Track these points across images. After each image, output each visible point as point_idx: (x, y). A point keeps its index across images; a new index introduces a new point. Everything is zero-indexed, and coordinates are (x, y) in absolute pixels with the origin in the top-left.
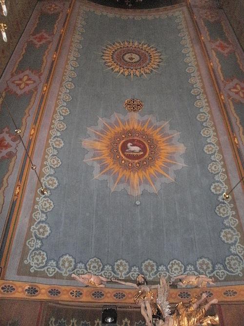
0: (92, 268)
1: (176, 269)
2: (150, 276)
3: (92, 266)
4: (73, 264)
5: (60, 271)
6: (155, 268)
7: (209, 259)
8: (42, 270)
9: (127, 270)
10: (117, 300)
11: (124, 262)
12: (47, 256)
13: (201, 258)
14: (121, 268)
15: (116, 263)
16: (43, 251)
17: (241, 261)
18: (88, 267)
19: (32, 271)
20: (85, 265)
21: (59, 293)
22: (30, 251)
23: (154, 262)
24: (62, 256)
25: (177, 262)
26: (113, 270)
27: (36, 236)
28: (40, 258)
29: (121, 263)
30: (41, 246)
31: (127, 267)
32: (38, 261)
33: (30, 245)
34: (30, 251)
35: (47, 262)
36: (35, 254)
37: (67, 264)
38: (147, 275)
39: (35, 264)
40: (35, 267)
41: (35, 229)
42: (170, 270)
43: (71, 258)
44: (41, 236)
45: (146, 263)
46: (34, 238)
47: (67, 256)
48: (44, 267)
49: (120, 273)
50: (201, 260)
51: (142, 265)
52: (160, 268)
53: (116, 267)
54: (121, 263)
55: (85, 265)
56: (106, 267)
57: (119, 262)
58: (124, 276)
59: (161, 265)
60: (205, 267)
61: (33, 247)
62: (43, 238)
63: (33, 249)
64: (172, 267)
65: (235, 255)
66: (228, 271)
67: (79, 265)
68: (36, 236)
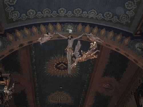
0: (45, 13)
1: (93, 14)
2: (77, 15)
3: (45, 12)
4: (35, 13)
5: (28, 17)
6: (81, 12)
7: (112, 13)
8: (19, 19)
9: (65, 12)
10: (59, 39)
11: (64, 9)
12: (19, 12)
13: (108, 11)
14: (62, 12)
15: (59, 10)
16: (17, 11)
17: (128, 19)
18: (43, 13)
19: (14, 20)
20: (42, 12)
21: (32, 41)
22: (10, 13)
23: (81, 9)
24: (28, 10)
25: (94, 11)
26: (57, 13)
27: (9, 5)
28: (16, 14)
29: (62, 10)
30: (14, 9)
31: (65, 11)
32: (15, 16)
33: (8, 10)
34: (10, 13)
35: (20, 15)
36: (12, 13)
37: (31, 14)
38: (76, 15)
39: (14, 17)
40: (15, 18)
41: (7, 2)
42: (89, 13)
43: (33, 10)
44: (13, 4)
45: (77, 9)
46: (9, 6)
47: (31, 10)
48: (20, 17)
49: (61, 14)
50: (108, 12)
51: (74, 11)
52: (84, 12)
53: (59, 11)
54: (62, 10)
55: (42, 12)
56: (53, 12)
57: (61, 9)
58: (63, 15)
59: (84, 11)
60: (108, 16)
61: (10, 11)
62: (14, 5)
63: (10, 11)
64: (91, 12)
65: (127, 15)
66: (119, 20)
67: (38, 13)
68: (9, 5)
